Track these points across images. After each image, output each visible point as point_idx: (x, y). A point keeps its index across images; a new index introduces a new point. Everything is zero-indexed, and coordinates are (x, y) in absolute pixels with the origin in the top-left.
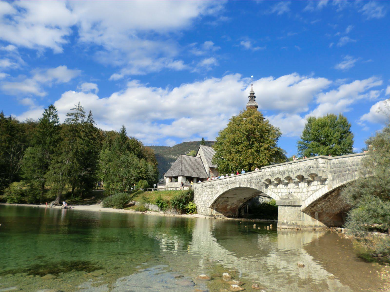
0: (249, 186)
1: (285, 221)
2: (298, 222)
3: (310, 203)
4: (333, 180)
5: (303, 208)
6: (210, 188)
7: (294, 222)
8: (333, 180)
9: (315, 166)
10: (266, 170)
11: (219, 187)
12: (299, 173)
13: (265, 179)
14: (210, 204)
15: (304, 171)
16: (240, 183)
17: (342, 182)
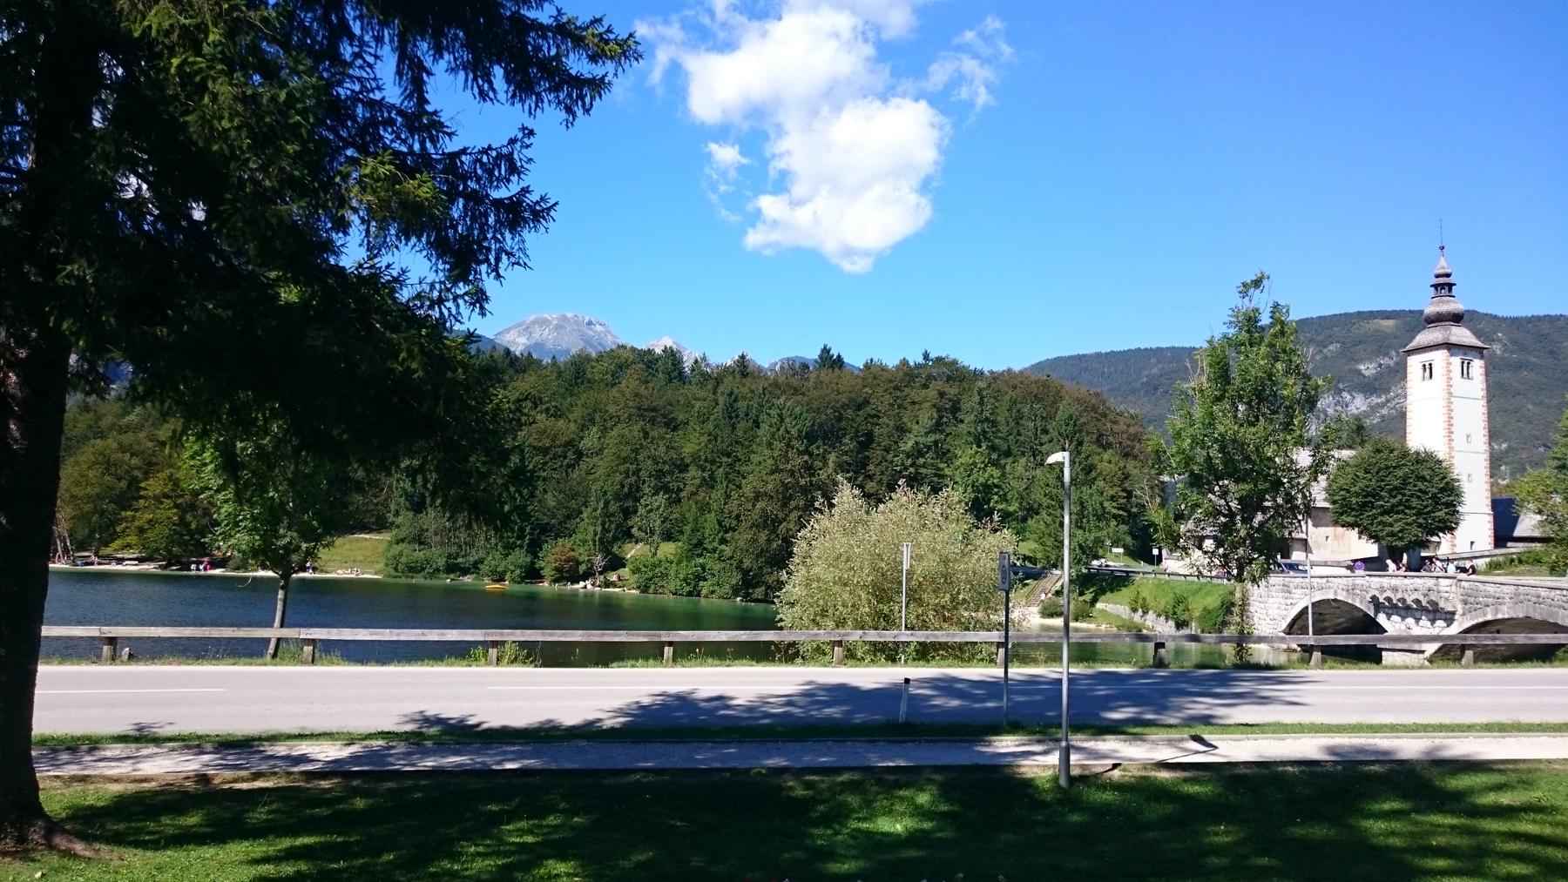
0: (1350, 601)
5: (1427, 654)
6: (1283, 591)
9: (1435, 588)
11: (1299, 591)
12: (1415, 596)
16: (1336, 593)
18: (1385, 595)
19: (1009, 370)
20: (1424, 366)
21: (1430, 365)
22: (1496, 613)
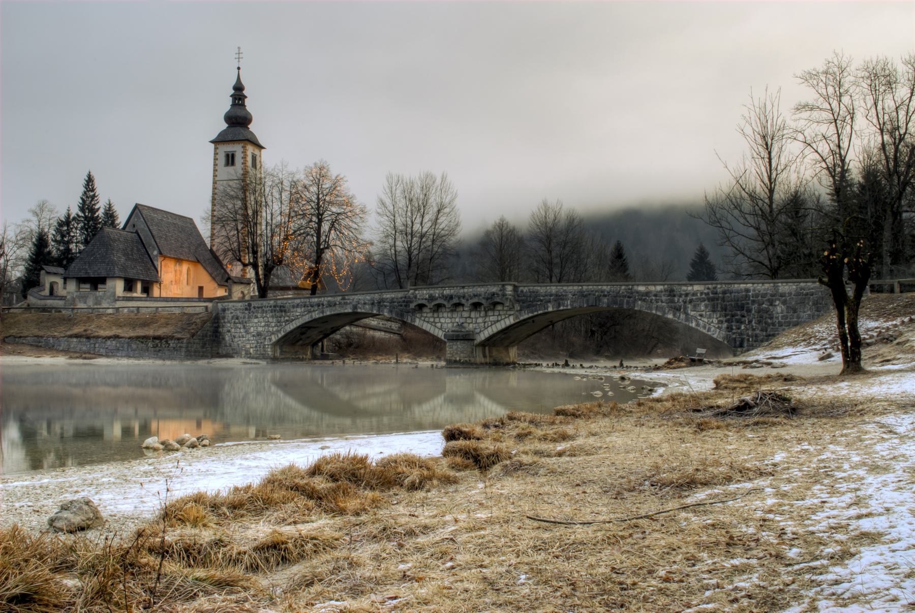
1: (458, 359)
2: (471, 359)
4: (521, 310)
5: (476, 342)
7: (467, 359)
8: (521, 310)
9: (500, 293)
10: (417, 292)
12: (476, 300)
13: (415, 304)
14: (274, 339)
15: (484, 298)
17: (532, 313)
18: (433, 304)
20: (227, 156)
21: (233, 156)
22: (559, 306)
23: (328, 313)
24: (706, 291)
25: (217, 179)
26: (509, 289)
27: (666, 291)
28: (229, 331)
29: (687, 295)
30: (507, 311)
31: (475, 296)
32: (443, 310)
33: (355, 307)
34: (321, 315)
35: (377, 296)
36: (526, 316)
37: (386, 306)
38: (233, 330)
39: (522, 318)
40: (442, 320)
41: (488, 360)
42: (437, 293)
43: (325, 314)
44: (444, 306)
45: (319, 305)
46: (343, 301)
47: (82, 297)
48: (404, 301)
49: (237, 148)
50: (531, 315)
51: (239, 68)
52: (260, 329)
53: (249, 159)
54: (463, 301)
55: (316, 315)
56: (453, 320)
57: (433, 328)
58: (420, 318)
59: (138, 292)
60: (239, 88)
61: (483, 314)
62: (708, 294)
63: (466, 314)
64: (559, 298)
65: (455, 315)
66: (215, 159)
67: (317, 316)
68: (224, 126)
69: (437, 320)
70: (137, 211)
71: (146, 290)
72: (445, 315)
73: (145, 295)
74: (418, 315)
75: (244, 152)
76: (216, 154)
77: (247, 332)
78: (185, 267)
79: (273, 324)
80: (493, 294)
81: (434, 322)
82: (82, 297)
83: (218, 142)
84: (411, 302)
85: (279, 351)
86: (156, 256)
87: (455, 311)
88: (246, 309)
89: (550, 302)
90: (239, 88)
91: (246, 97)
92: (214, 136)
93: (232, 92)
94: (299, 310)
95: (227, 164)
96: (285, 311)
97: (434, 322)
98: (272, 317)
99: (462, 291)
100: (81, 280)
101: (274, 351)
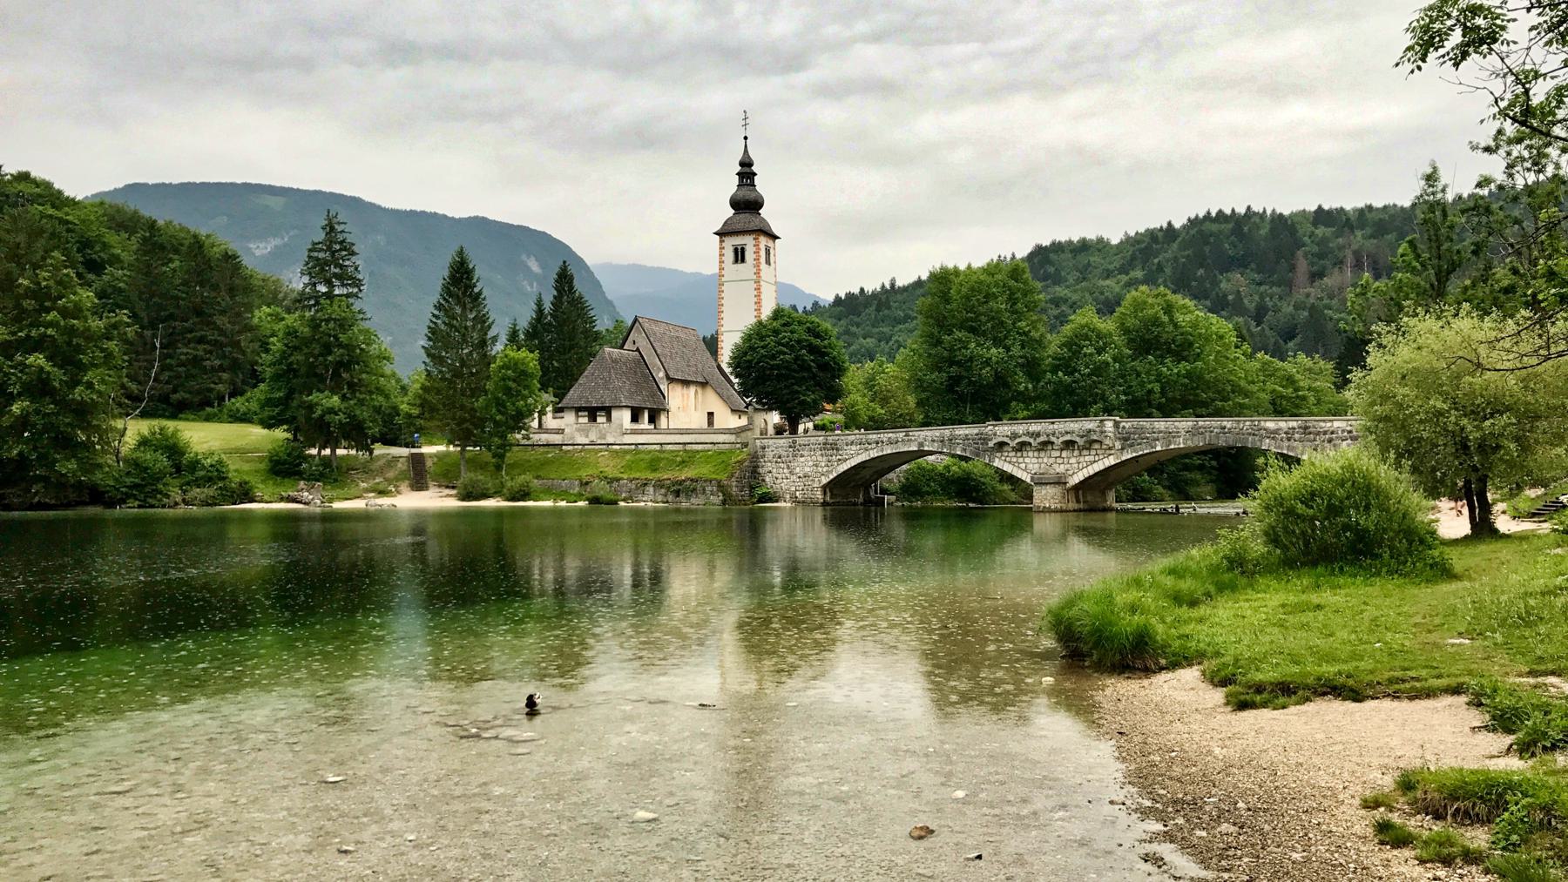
3: (1082, 478)
4: (1123, 449)
8: (1123, 449)
10: (997, 428)
12: (1068, 437)
13: (995, 441)
14: (825, 480)
15: (1078, 436)
19: (1342, 209)
20: (736, 250)
21: (743, 250)
22: (1170, 444)
23: (889, 452)
24: (1349, 428)
25: (723, 279)
26: (1109, 425)
27: (1300, 427)
28: (770, 472)
29: (1325, 433)
30: (1105, 450)
31: (1067, 433)
32: (1028, 449)
33: (921, 444)
34: (881, 454)
35: (947, 433)
36: (1129, 456)
37: (958, 444)
38: (774, 470)
39: (1124, 458)
40: (1027, 460)
41: (1081, 506)
42: (1020, 428)
43: (885, 453)
44: (1030, 444)
45: (877, 443)
46: (906, 438)
47: (583, 430)
48: (980, 439)
49: (748, 241)
50: (1134, 455)
51: (746, 138)
52: (807, 469)
53: (763, 253)
54: (1053, 439)
55: (874, 454)
56: (1040, 460)
57: (1015, 469)
58: (1000, 458)
59: (645, 424)
60: (746, 164)
61: (1076, 453)
62: (1350, 432)
63: (1058, 454)
64: (1170, 435)
65: (1042, 454)
66: (721, 255)
67: (876, 455)
68: (731, 212)
69: (1021, 460)
70: (637, 324)
71: (652, 420)
72: (1031, 454)
73: (652, 427)
74: (998, 454)
75: (756, 246)
76: (722, 248)
77: (791, 473)
78: (692, 389)
79: (823, 464)
80: (1090, 431)
81: (1017, 462)
82: (583, 430)
83: (722, 234)
84: (990, 440)
85: (828, 494)
86: (662, 378)
87: (1043, 450)
88: (790, 447)
89: (1158, 440)
90: (746, 164)
91: (755, 174)
92: (718, 227)
93: (738, 168)
94: (854, 447)
95: (736, 261)
96: (837, 449)
97: (1017, 462)
98: (822, 455)
99: (1051, 426)
100: (578, 410)
101: (825, 493)
